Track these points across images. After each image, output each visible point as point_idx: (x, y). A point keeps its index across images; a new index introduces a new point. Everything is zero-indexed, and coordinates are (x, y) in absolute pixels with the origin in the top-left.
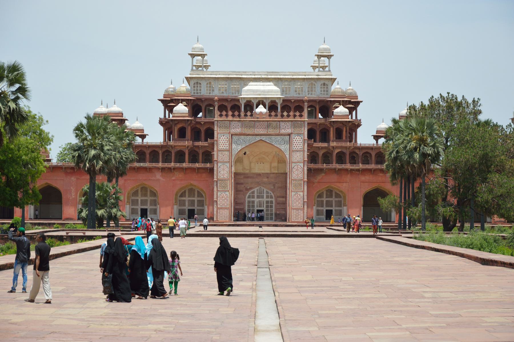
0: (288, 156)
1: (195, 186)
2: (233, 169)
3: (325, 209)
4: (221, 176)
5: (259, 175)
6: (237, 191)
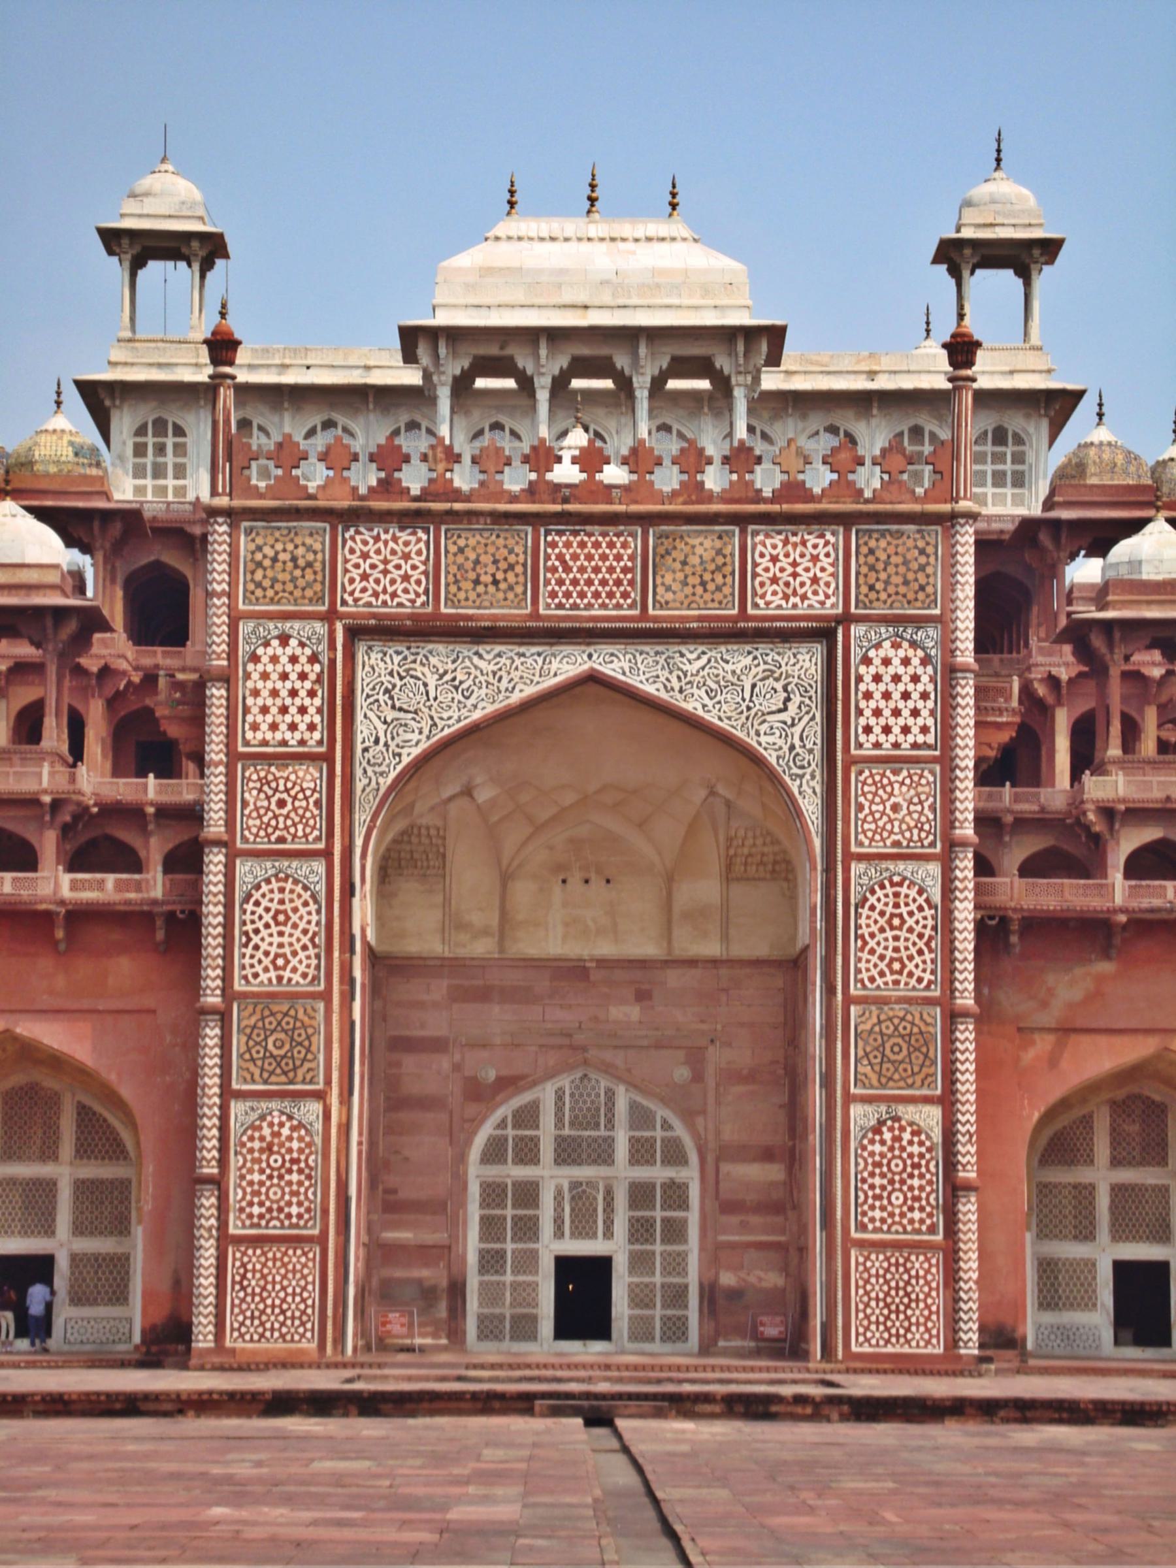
0: (811, 808)
1: (56, 1062)
2: (363, 910)
3: (1104, 1254)
4: (256, 973)
5: (574, 973)
6: (393, 1105)
